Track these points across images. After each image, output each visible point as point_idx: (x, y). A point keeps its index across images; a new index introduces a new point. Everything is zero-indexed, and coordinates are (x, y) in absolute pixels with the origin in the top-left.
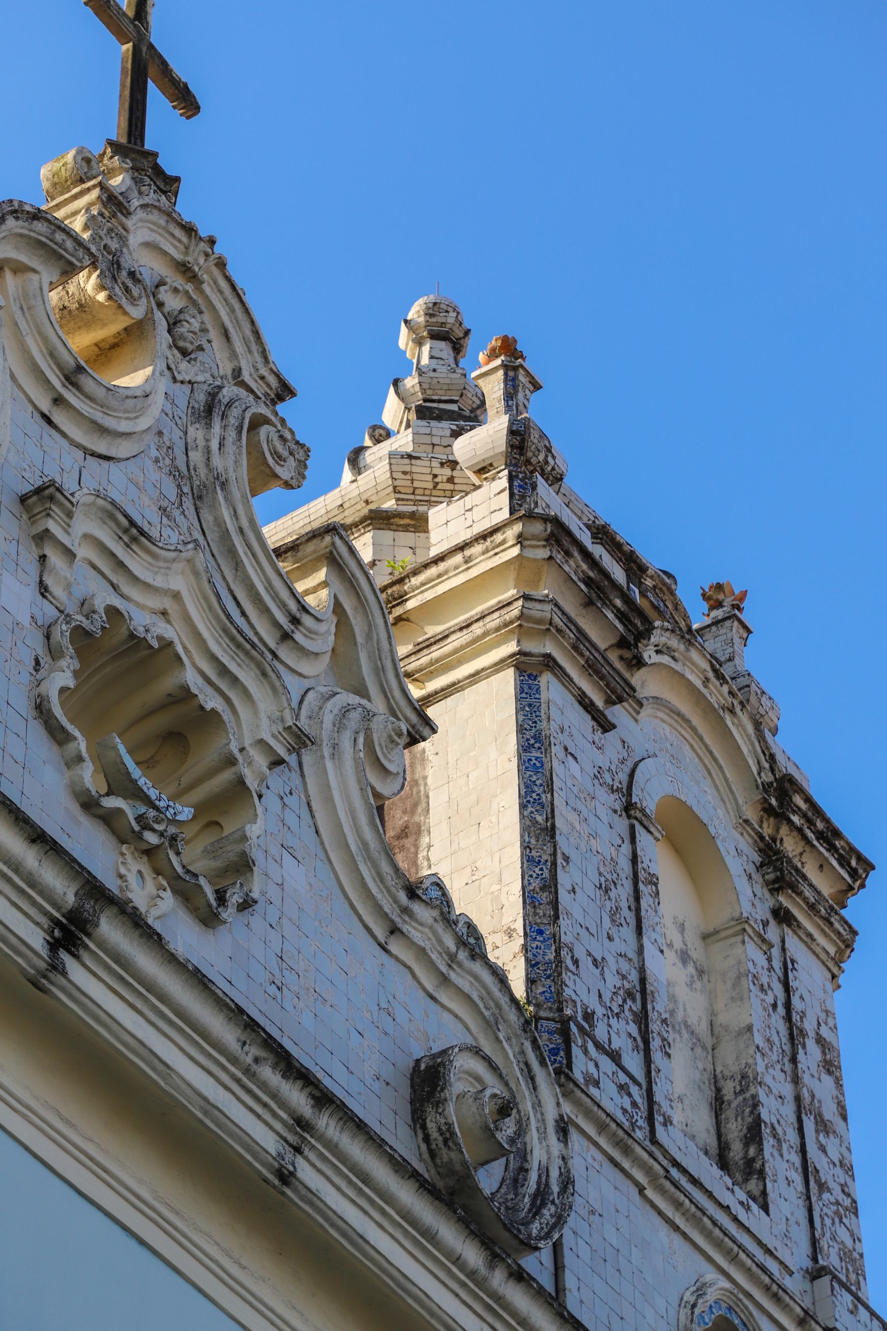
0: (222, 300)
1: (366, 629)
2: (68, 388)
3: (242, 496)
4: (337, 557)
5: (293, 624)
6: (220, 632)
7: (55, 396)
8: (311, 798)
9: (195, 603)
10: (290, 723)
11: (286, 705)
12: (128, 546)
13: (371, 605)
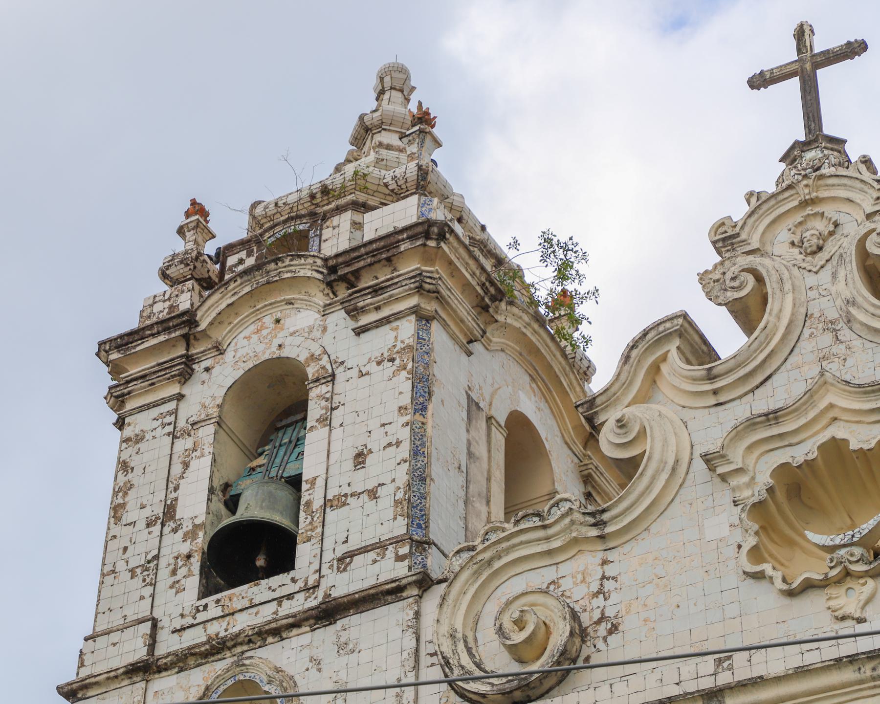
0: (837, 188)
6: (865, 396)
7: (712, 392)
9: (842, 398)
12: (778, 423)
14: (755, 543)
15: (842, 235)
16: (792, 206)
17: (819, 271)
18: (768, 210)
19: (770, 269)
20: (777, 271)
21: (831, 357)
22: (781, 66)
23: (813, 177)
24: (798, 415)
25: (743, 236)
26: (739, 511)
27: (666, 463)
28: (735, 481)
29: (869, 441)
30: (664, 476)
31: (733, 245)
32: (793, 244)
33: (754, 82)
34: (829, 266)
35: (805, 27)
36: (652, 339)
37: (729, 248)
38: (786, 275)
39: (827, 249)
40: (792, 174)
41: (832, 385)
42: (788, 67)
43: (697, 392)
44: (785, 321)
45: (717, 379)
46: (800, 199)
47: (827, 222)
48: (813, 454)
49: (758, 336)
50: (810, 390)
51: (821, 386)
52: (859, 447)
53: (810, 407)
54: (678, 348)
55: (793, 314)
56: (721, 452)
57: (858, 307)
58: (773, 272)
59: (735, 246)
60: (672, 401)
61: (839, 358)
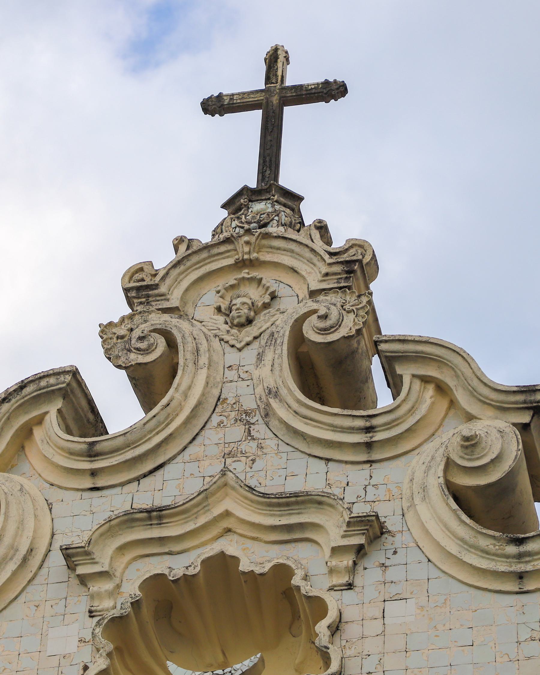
1: (453, 373)
2: (95, 460)
3: (288, 390)
4: (393, 354)
5: (369, 432)
6: (268, 508)
7: (89, 472)
8: (417, 541)
9: (242, 506)
10: (347, 519)
11: (342, 509)
12: (160, 524)
13: (445, 356)
14: (104, 667)
15: (277, 310)
16: (227, 264)
17: (243, 348)
18: (198, 262)
19: (187, 335)
20: (195, 339)
21: (239, 455)
22: (244, 93)
23: (257, 234)
24: (186, 518)
25: (163, 289)
26: (94, 624)
27: (17, 550)
28: (96, 587)
29: (263, 563)
30: (12, 566)
31: (149, 297)
32: (219, 309)
33: (209, 105)
34: (256, 345)
35: (279, 52)
36: (29, 395)
37: (144, 300)
38: (204, 346)
39: (258, 324)
40: (234, 225)
41: (233, 488)
42: (252, 96)
43: (71, 469)
44: (192, 402)
45: (99, 458)
46: (237, 257)
47: (264, 292)
48: (194, 568)
49: (157, 414)
50: (206, 490)
51: (220, 488)
52: (250, 569)
53: (202, 511)
54: (59, 411)
55: (203, 394)
56: (86, 548)
57: (281, 401)
58: (190, 339)
59: (151, 299)
60: (40, 475)
61: (247, 457)
